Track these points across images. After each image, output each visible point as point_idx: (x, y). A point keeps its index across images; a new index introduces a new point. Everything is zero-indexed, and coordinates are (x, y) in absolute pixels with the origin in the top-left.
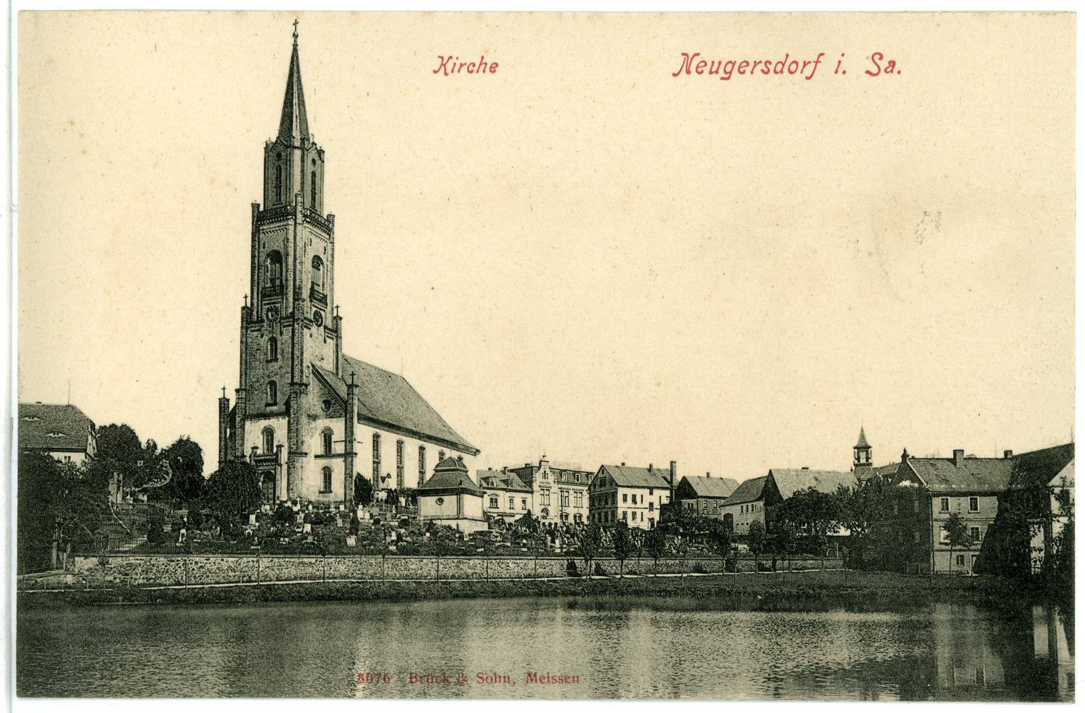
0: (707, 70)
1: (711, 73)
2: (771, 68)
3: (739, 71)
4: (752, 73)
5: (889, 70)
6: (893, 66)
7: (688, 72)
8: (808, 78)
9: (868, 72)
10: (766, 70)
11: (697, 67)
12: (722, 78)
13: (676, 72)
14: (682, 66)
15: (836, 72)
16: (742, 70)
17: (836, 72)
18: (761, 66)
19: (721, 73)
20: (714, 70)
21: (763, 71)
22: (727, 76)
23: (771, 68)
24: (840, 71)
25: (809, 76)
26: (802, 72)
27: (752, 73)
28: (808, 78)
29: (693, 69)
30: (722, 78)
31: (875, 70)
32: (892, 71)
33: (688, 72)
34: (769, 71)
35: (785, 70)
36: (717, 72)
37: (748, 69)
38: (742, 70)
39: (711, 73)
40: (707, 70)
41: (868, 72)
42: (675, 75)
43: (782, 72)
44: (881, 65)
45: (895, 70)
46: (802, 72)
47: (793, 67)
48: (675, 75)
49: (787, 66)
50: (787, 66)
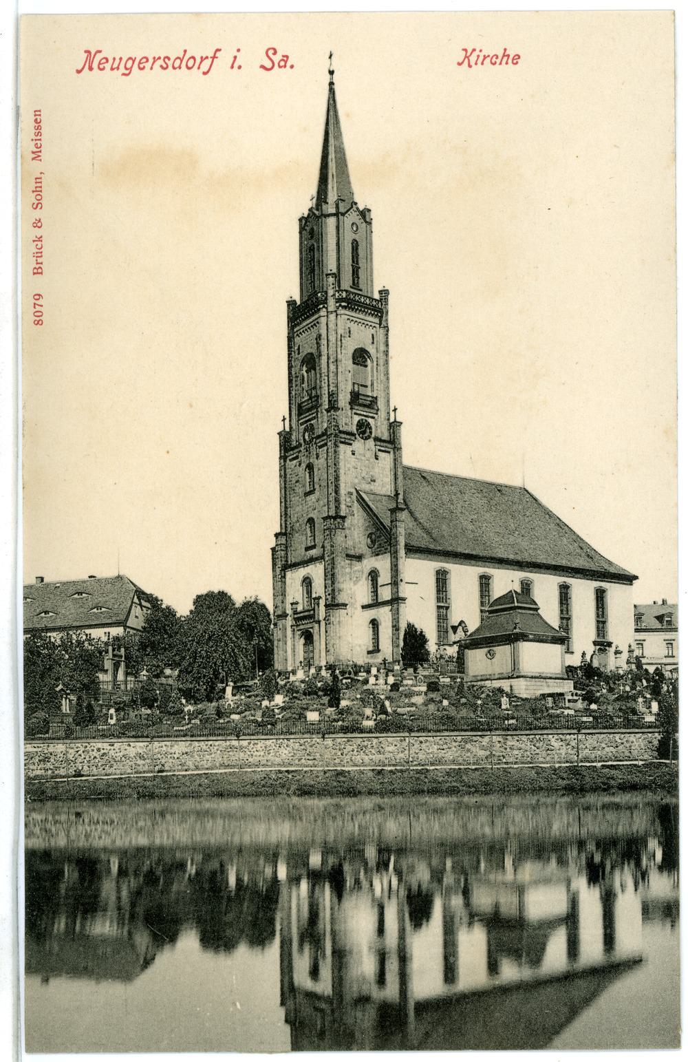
0: (108, 66)
1: (112, 69)
3: (139, 65)
4: (151, 68)
7: (91, 69)
8: (205, 73)
9: (263, 67)
10: (165, 66)
11: (100, 64)
12: (124, 74)
13: (80, 68)
14: (85, 65)
15: (232, 67)
16: (142, 66)
17: (232, 67)
19: (122, 70)
20: (115, 65)
21: (161, 66)
22: (127, 72)
24: (236, 65)
25: (206, 70)
26: (199, 68)
27: (151, 68)
28: (205, 73)
29: (95, 65)
30: (124, 74)
31: (269, 65)
32: (285, 66)
33: (91, 69)
34: (167, 67)
36: (118, 68)
37: (148, 65)
38: (142, 66)
39: (112, 69)
40: (108, 66)
41: (263, 67)
43: (180, 67)
45: (289, 64)
46: (199, 68)
48: (79, 72)
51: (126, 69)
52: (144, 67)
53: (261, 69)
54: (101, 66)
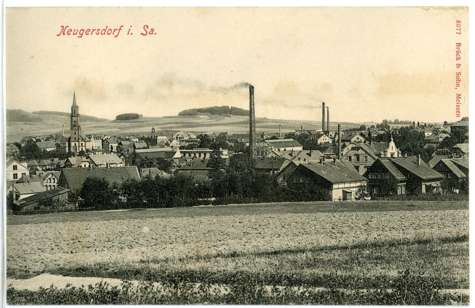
0: (72, 33)
2: (100, 32)
3: (86, 33)
4: (92, 34)
5: (151, 33)
6: (153, 31)
7: (64, 34)
8: (116, 36)
9: (142, 34)
10: (98, 33)
11: (68, 32)
12: (79, 37)
13: (58, 34)
15: (128, 34)
16: (87, 33)
17: (128, 34)
18: (96, 31)
19: (78, 35)
20: (75, 33)
21: (96, 33)
22: (81, 36)
23: (100, 32)
24: (130, 33)
25: (116, 35)
26: (113, 34)
27: (92, 34)
28: (116, 36)
29: (66, 33)
30: (79, 37)
31: (145, 33)
32: (152, 34)
33: (64, 34)
34: (99, 33)
35: (106, 33)
37: (90, 33)
38: (87, 33)
40: (72, 33)
41: (142, 34)
42: (58, 35)
43: (104, 34)
44: (148, 31)
45: (154, 33)
46: (113, 34)
47: (109, 32)
48: (58, 35)
49: (107, 31)
50: (107, 31)
51: (80, 34)
52: (88, 34)
53: (142, 35)
54: (69, 33)
